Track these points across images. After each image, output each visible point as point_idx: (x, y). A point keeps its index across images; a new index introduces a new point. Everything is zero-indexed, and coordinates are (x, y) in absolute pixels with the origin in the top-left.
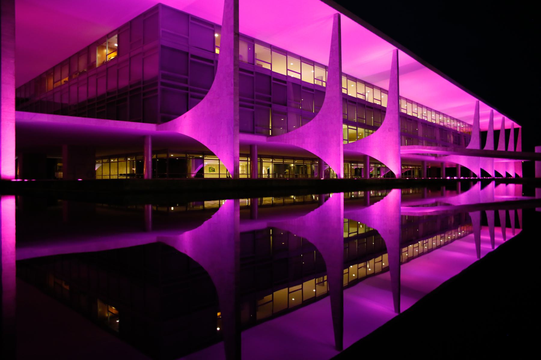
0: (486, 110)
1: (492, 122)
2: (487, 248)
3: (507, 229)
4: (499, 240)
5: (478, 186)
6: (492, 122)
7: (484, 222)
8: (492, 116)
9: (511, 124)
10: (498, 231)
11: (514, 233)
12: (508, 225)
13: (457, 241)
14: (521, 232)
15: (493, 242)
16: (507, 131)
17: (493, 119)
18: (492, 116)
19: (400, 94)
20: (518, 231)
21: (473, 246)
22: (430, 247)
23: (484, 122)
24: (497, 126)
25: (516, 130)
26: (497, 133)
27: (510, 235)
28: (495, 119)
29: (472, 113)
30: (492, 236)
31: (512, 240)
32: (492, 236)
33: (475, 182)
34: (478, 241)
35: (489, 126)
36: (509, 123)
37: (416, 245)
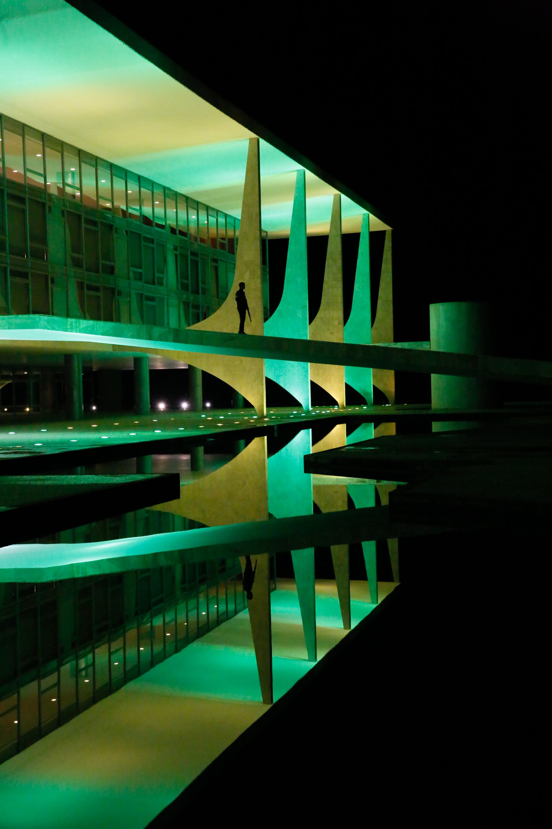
0: (281, 169)
1: (300, 213)
2: (294, 663)
3: (355, 588)
4: (332, 626)
5: (259, 444)
6: (300, 213)
7: (283, 571)
8: (302, 190)
9: (361, 218)
10: (326, 593)
12: (357, 572)
13: (195, 649)
14: (397, 588)
15: (310, 633)
16: (350, 241)
17: (303, 200)
18: (302, 190)
19: (21, 138)
20: (386, 589)
21: (246, 658)
22: (102, 680)
23: (277, 216)
24: (318, 224)
25: (376, 238)
27: (364, 604)
28: (310, 201)
29: (237, 178)
30: (309, 615)
31: (369, 622)
32: (309, 615)
33: (249, 434)
34: (264, 639)
35: (293, 227)
36: (356, 216)
37: (49, 681)
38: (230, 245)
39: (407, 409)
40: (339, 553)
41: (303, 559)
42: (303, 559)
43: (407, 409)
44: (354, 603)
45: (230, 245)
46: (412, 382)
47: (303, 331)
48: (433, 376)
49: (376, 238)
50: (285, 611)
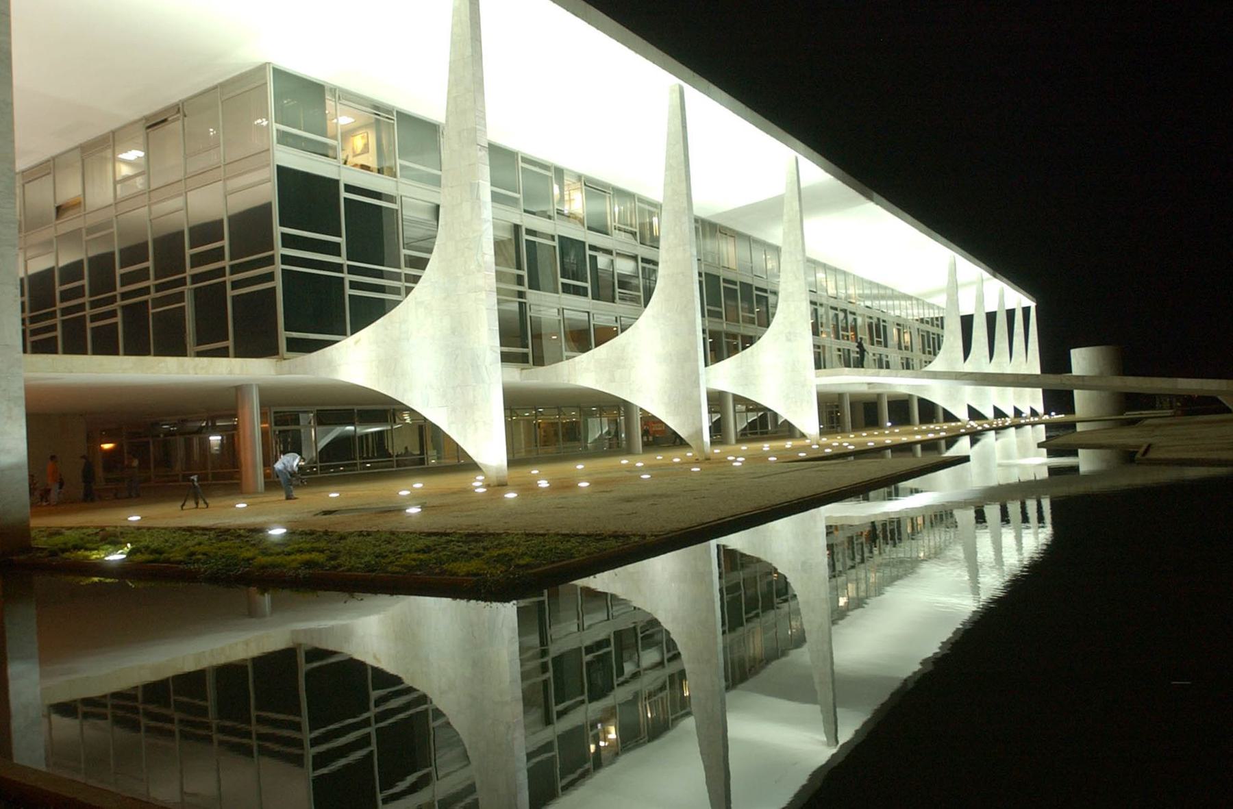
1: (980, 299)
6: (980, 299)
10: (1008, 536)
11: (1036, 534)
16: (1011, 314)
25: (1026, 311)
26: (991, 318)
29: (943, 281)
36: (1018, 299)
38: (940, 322)
39: (1055, 417)
40: (1014, 508)
41: (992, 512)
42: (992, 512)
43: (1055, 417)
44: (1024, 541)
45: (940, 322)
46: (1058, 400)
47: (1009, 369)
48: (1076, 392)
49: (1026, 311)
50: (984, 542)
